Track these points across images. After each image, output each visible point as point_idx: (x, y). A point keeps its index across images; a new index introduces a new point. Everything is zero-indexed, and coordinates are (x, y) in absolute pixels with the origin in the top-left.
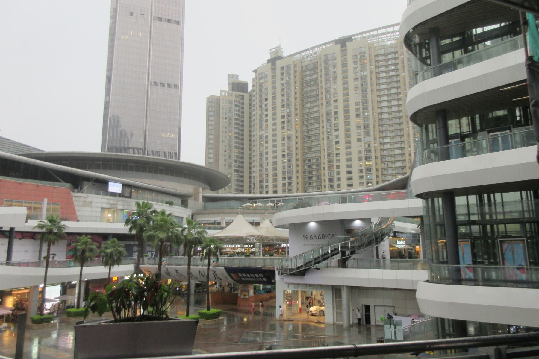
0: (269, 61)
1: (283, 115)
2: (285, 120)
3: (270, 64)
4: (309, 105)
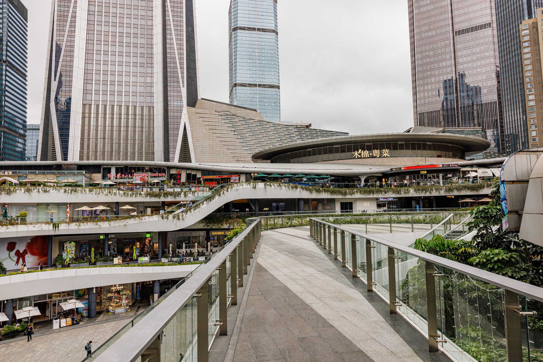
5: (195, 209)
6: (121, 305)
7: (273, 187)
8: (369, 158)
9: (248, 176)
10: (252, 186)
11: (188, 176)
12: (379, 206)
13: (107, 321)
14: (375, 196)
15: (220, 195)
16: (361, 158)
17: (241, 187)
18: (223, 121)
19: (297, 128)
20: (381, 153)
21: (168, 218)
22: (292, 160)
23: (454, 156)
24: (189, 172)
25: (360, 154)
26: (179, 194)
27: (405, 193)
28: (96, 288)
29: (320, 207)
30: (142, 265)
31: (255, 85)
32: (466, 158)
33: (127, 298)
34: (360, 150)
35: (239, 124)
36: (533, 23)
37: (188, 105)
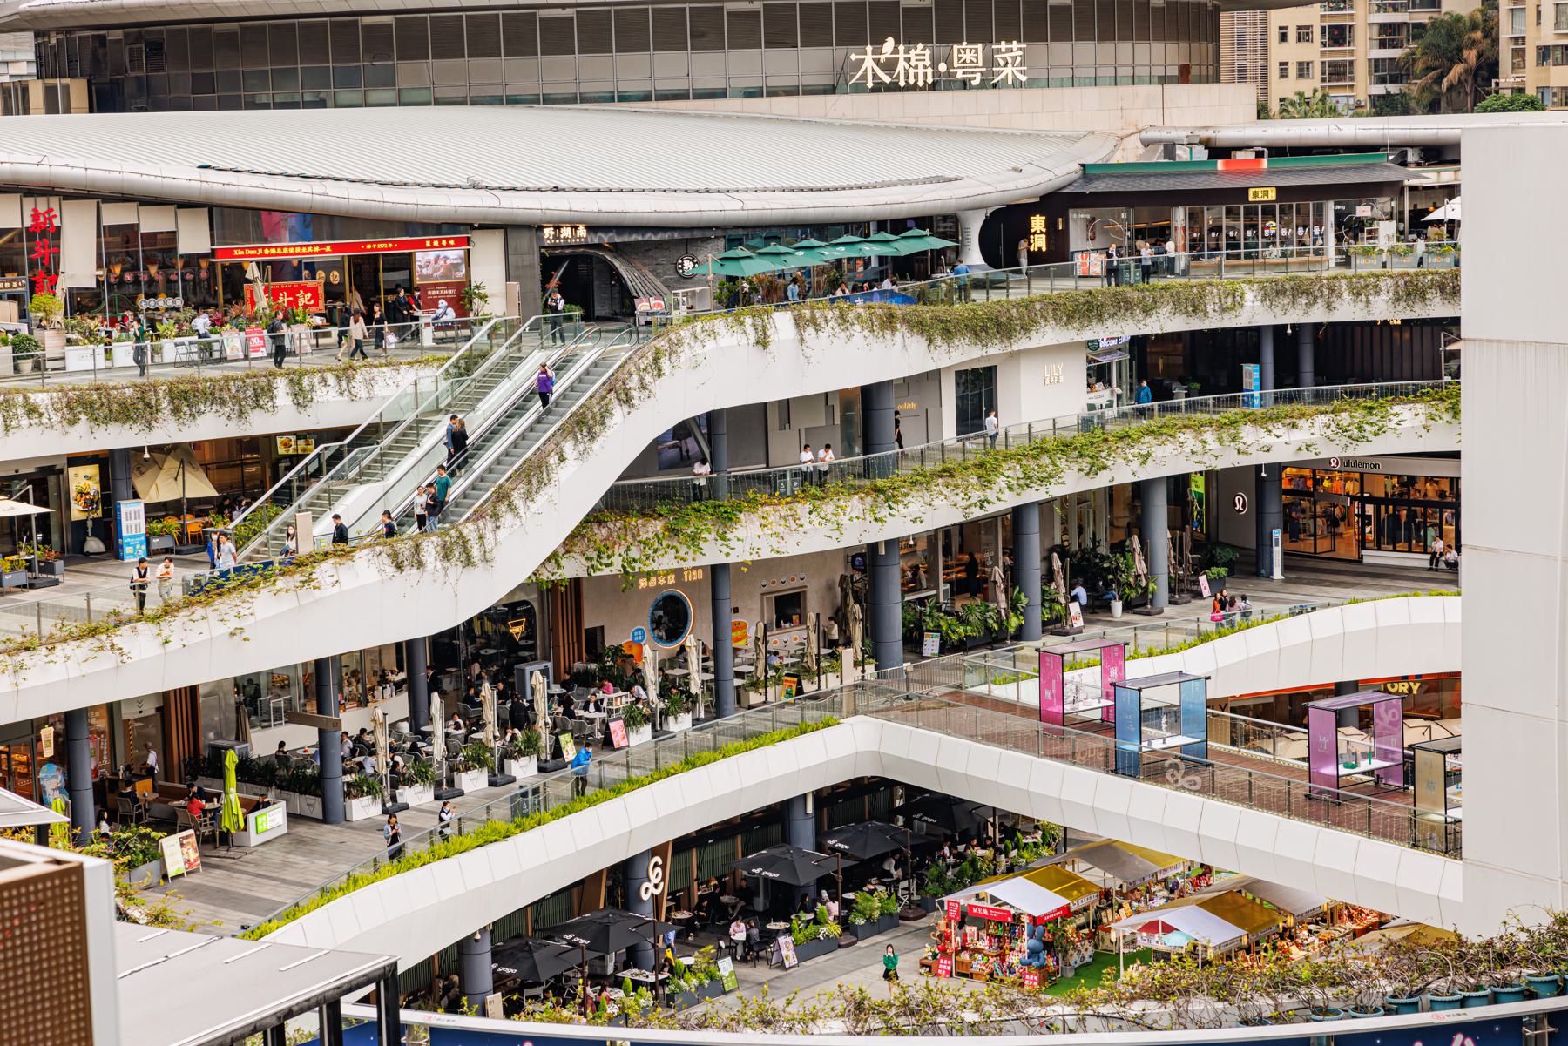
5: (529, 495)
8: (933, 87)
9: (523, 240)
10: (753, 339)
11: (119, 245)
12: (1099, 374)
15: (628, 401)
16: (893, 88)
17: (710, 344)
20: (990, 62)
21: (420, 564)
24: (116, 216)
25: (889, 66)
27: (1224, 310)
34: (890, 43)
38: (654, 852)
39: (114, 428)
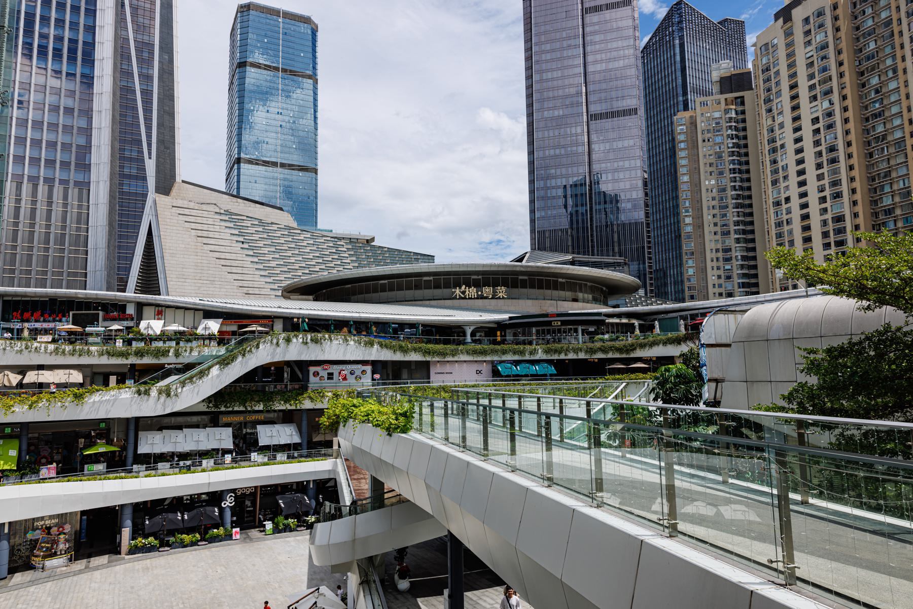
0: (777, 17)
1: (815, 115)
2: (821, 125)
3: (781, 21)
4: (875, 81)
6: (56, 552)
7: (335, 342)
13: (32, 583)
14: (488, 358)
15: (244, 355)
16: (465, 298)
18: (223, 224)
19: (351, 242)
20: (495, 292)
22: (352, 298)
23: (595, 300)
25: (463, 293)
26: (165, 353)
28: (10, 523)
29: (405, 374)
30: (94, 476)
31: (275, 164)
32: (610, 303)
33: (67, 541)
35: (252, 230)
36: (691, 117)
37: (158, 190)
38: (233, 491)
39: (114, 358)
